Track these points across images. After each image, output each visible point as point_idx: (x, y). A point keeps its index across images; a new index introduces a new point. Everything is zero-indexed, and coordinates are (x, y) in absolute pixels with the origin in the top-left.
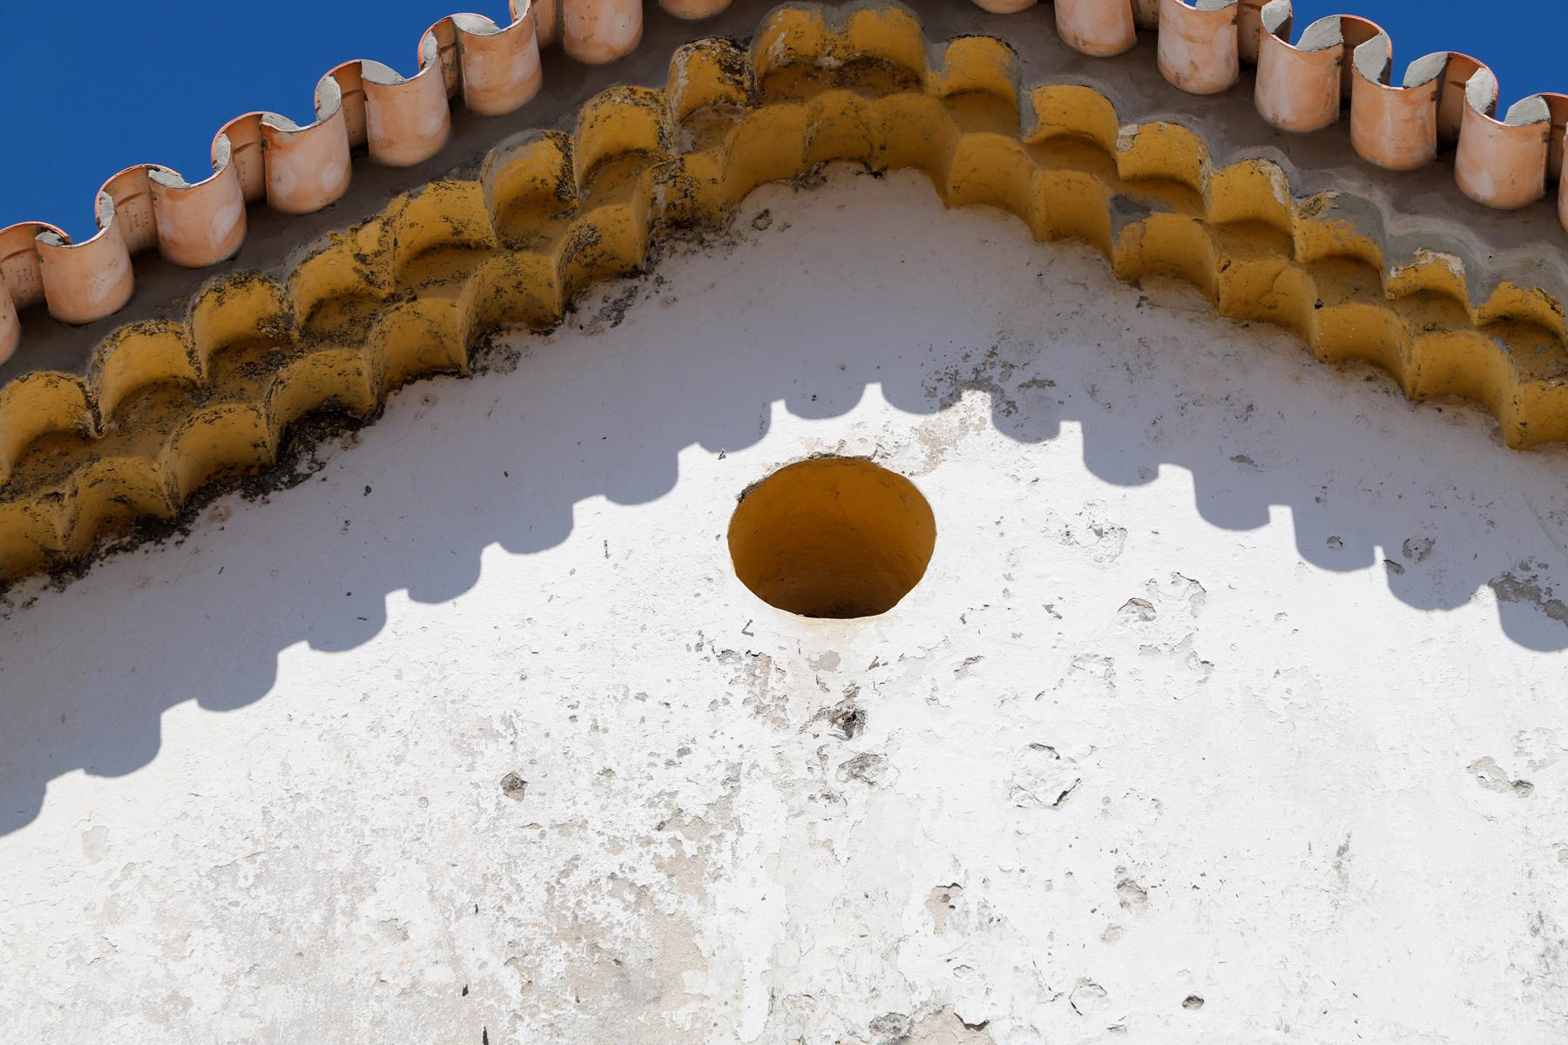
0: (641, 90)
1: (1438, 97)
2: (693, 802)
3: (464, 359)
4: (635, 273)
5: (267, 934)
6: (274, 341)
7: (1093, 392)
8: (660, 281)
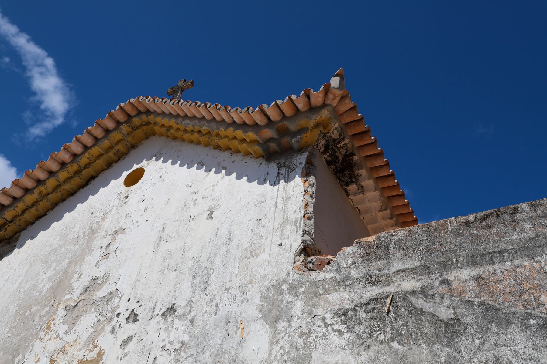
3: (106, 168)
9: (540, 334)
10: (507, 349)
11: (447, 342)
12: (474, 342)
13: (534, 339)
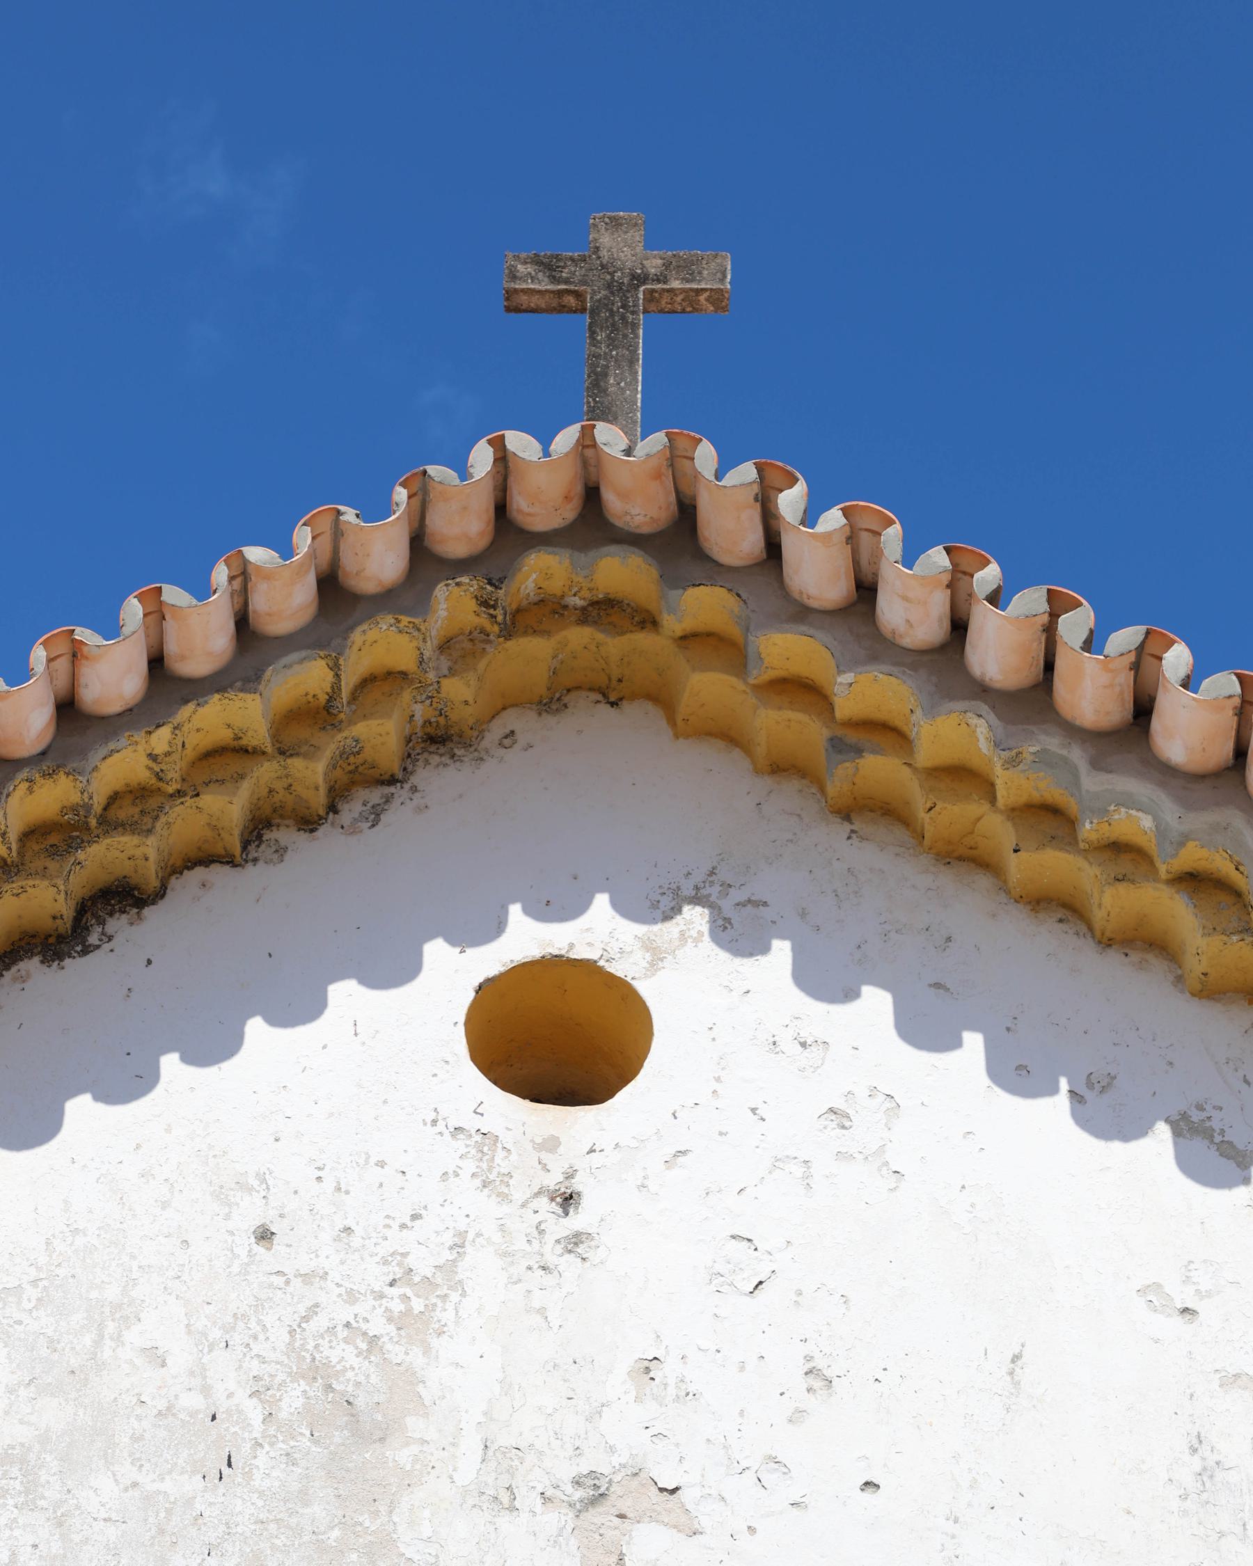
0: (405, 620)
1: (1136, 667)
2: (423, 1264)
3: (237, 850)
4: (392, 781)
5: (44, 1352)
6: (74, 827)
7: (803, 914)
8: (414, 789)
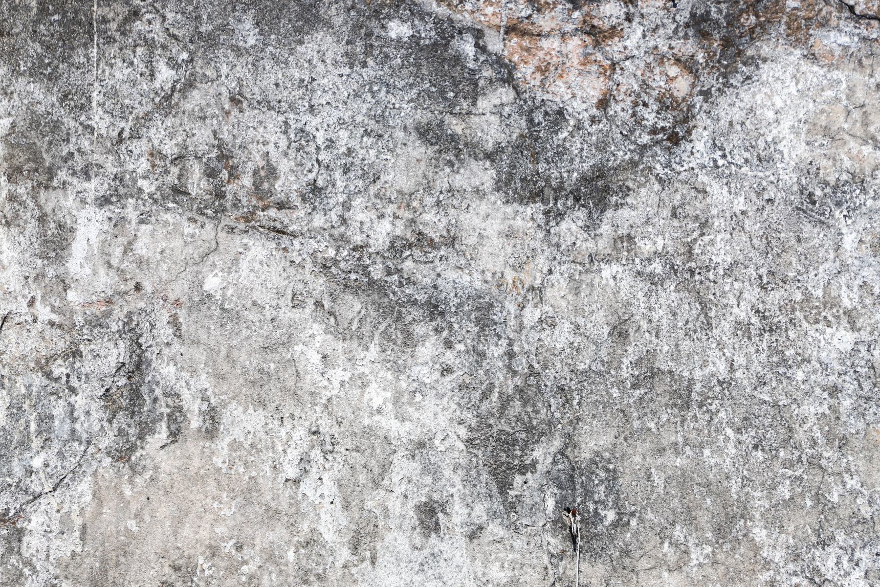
9: (411, 81)
10: (273, 121)
11: (40, 57)
12: (152, 75)
13: (383, 93)
